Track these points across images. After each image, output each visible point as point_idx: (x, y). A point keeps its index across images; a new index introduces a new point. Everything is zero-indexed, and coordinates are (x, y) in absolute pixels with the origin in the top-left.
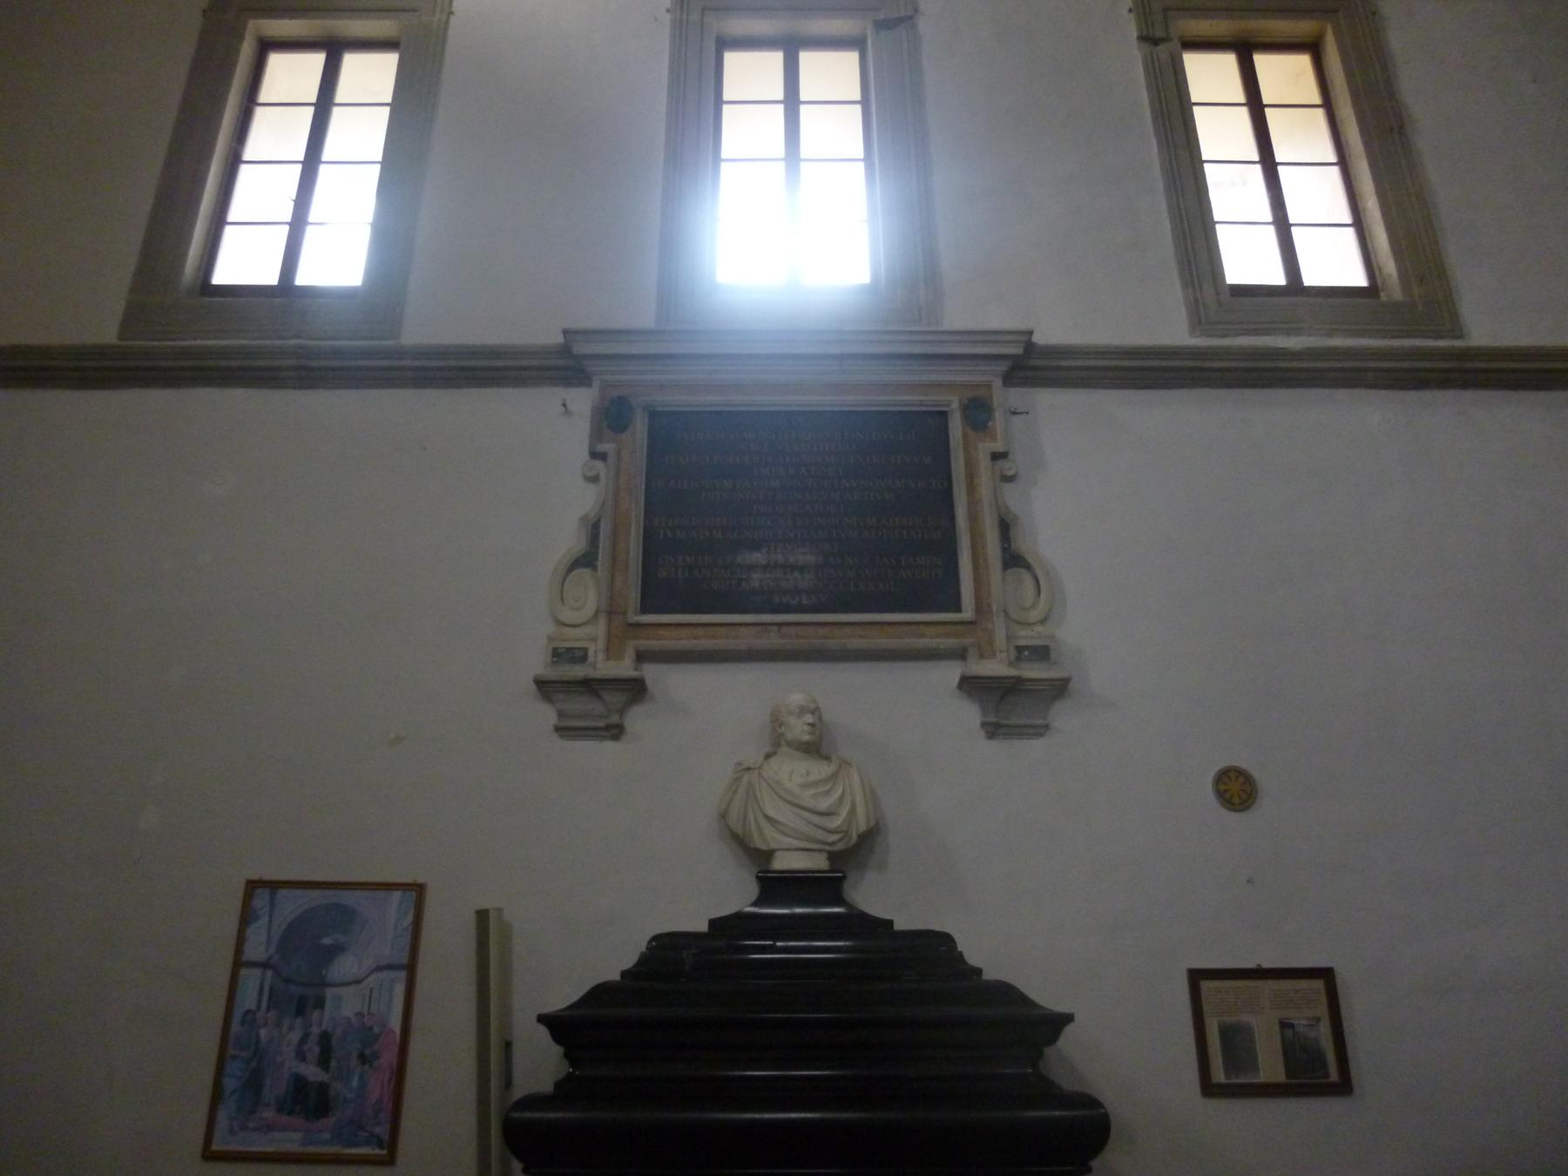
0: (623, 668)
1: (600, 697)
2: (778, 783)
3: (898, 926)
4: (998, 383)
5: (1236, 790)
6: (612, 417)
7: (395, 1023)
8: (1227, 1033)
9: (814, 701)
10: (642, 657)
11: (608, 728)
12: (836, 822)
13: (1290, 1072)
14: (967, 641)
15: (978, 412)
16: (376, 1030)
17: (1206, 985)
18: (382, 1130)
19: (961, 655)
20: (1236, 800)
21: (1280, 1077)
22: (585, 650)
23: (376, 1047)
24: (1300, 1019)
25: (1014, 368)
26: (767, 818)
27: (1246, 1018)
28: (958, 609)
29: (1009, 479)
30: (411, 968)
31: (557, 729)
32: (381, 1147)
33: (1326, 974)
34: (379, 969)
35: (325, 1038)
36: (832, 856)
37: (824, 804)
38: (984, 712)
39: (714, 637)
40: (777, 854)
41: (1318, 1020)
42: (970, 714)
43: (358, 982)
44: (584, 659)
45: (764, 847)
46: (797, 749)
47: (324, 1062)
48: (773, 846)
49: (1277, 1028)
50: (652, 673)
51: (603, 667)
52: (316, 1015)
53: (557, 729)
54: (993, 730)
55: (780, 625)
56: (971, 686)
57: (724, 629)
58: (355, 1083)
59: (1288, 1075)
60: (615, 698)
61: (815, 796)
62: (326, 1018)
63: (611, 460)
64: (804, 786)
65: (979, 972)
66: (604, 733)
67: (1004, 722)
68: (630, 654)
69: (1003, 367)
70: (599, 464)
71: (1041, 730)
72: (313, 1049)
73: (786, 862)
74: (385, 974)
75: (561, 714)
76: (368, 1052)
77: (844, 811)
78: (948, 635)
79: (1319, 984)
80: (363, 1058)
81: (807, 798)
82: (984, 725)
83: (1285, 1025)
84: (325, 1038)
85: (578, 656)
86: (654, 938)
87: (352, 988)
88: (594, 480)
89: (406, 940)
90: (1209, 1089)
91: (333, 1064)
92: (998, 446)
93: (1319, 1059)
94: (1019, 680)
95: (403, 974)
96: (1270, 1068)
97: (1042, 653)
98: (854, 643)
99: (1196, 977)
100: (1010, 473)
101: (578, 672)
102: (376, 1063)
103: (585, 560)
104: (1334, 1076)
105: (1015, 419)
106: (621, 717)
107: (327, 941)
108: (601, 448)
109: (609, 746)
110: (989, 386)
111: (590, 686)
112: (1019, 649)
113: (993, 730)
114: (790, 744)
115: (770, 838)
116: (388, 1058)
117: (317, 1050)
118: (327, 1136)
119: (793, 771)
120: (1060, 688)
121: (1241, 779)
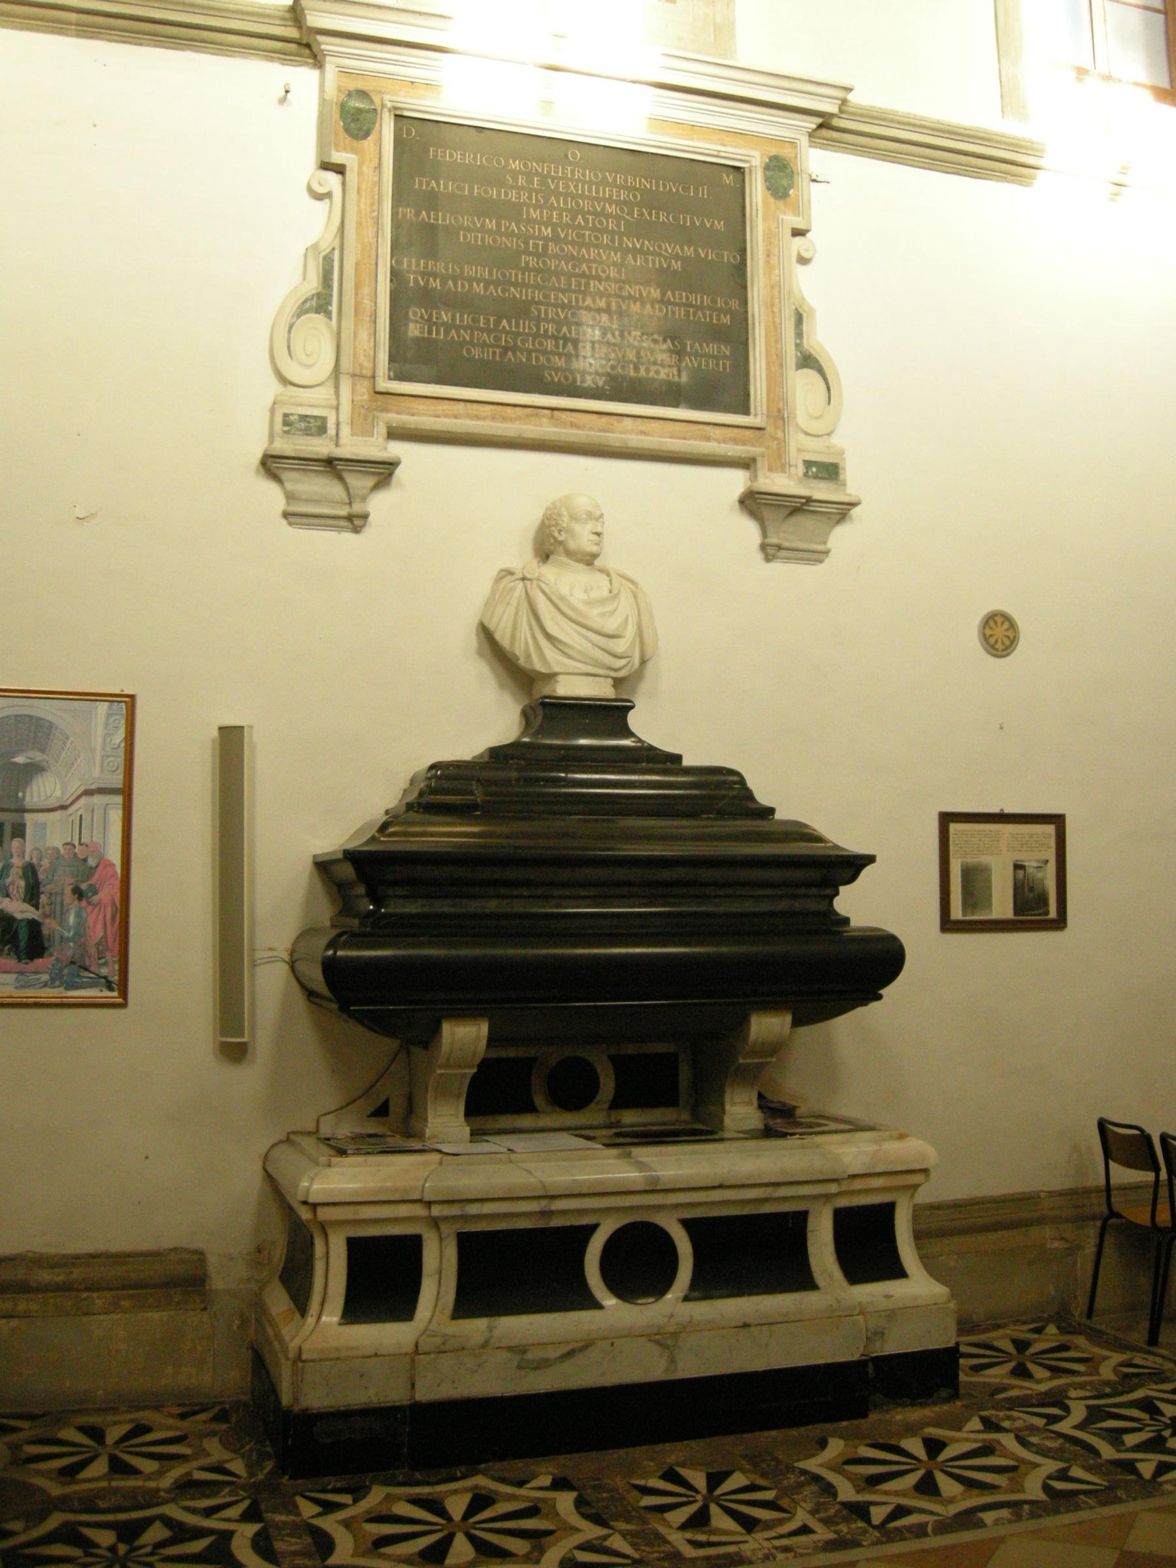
0: (374, 447)
1: (341, 479)
2: (562, 598)
3: (687, 762)
4: (804, 140)
5: (999, 634)
6: (353, 117)
7: (114, 855)
8: (968, 874)
9: (598, 506)
11: (350, 518)
12: (620, 646)
13: (1019, 908)
15: (781, 175)
16: (92, 862)
17: (954, 827)
18: (110, 970)
19: (747, 464)
20: (999, 646)
22: (324, 420)
23: (93, 881)
24: (1031, 864)
25: (821, 126)
26: (549, 637)
27: (985, 859)
28: (745, 409)
30: (127, 792)
31: (286, 515)
32: (111, 989)
33: (1058, 821)
34: (88, 793)
35: (30, 871)
36: (618, 683)
37: (610, 626)
38: (765, 534)
39: (478, 418)
40: (560, 678)
41: (1047, 862)
42: (749, 531)
43: (64, 807)
44: (322, 430)
45: (543, 670)
46: (577, 561)
47: (33, 894)
48: (557, 669)
49: (1012, 867)
51: (352, 446)
52: (16, 843)
53: (286, 515)
54: (769, 551)
55: (552, 409)
56: (752, 503)
57: (488, 407)
58: (72, 919)
59: (1015, 914)
60: (359, 482)
61: (603, 615)
62: (28, 849)
64: (590, 603)
65: (767, 813)
67: (786, 544)
68: (381, 430)
69: (811, 123)
70: (333, 179)
71: (818, 556)
72: (20, 885)
73: (570, 687)
74: (96, 799)
75: (290, 497)
76: (84, 886)
77: (630, 631)
78: (736, 441)
79: (1050, 829)
80: (79, 893)
81: (594, 616)
82: (763, 547)
83: (1018, 867)
84: (30, 871)
85: (318, 427)
86: (433, 767)
87: (57, 815)
89: (120, 760)
90: (948, 925)
91: (43, 899)
92: (800, 224)
93: (1043, 900)
94: (809, 500)
95: (119, 799)
96: (1002, 906)
98: (636, 441)
99: (947, 819)
101: (320, 447)
102: (95, 899)
103: (320, 303)
104: (1053, 914)
105: (813, 185)
107: (20, 759)
108: (337, 157)
109: (348, 536)
110: (793, 144)
111: (331, 465)
112: (808, 464)
113: (769, 551)
114: (569, 553)
115: (554, 660)
116: (108, 893)
117: (22, 883)
118: (45, 977)
119: (568, 581)
120: (842, 511)
121: (1006, 625)
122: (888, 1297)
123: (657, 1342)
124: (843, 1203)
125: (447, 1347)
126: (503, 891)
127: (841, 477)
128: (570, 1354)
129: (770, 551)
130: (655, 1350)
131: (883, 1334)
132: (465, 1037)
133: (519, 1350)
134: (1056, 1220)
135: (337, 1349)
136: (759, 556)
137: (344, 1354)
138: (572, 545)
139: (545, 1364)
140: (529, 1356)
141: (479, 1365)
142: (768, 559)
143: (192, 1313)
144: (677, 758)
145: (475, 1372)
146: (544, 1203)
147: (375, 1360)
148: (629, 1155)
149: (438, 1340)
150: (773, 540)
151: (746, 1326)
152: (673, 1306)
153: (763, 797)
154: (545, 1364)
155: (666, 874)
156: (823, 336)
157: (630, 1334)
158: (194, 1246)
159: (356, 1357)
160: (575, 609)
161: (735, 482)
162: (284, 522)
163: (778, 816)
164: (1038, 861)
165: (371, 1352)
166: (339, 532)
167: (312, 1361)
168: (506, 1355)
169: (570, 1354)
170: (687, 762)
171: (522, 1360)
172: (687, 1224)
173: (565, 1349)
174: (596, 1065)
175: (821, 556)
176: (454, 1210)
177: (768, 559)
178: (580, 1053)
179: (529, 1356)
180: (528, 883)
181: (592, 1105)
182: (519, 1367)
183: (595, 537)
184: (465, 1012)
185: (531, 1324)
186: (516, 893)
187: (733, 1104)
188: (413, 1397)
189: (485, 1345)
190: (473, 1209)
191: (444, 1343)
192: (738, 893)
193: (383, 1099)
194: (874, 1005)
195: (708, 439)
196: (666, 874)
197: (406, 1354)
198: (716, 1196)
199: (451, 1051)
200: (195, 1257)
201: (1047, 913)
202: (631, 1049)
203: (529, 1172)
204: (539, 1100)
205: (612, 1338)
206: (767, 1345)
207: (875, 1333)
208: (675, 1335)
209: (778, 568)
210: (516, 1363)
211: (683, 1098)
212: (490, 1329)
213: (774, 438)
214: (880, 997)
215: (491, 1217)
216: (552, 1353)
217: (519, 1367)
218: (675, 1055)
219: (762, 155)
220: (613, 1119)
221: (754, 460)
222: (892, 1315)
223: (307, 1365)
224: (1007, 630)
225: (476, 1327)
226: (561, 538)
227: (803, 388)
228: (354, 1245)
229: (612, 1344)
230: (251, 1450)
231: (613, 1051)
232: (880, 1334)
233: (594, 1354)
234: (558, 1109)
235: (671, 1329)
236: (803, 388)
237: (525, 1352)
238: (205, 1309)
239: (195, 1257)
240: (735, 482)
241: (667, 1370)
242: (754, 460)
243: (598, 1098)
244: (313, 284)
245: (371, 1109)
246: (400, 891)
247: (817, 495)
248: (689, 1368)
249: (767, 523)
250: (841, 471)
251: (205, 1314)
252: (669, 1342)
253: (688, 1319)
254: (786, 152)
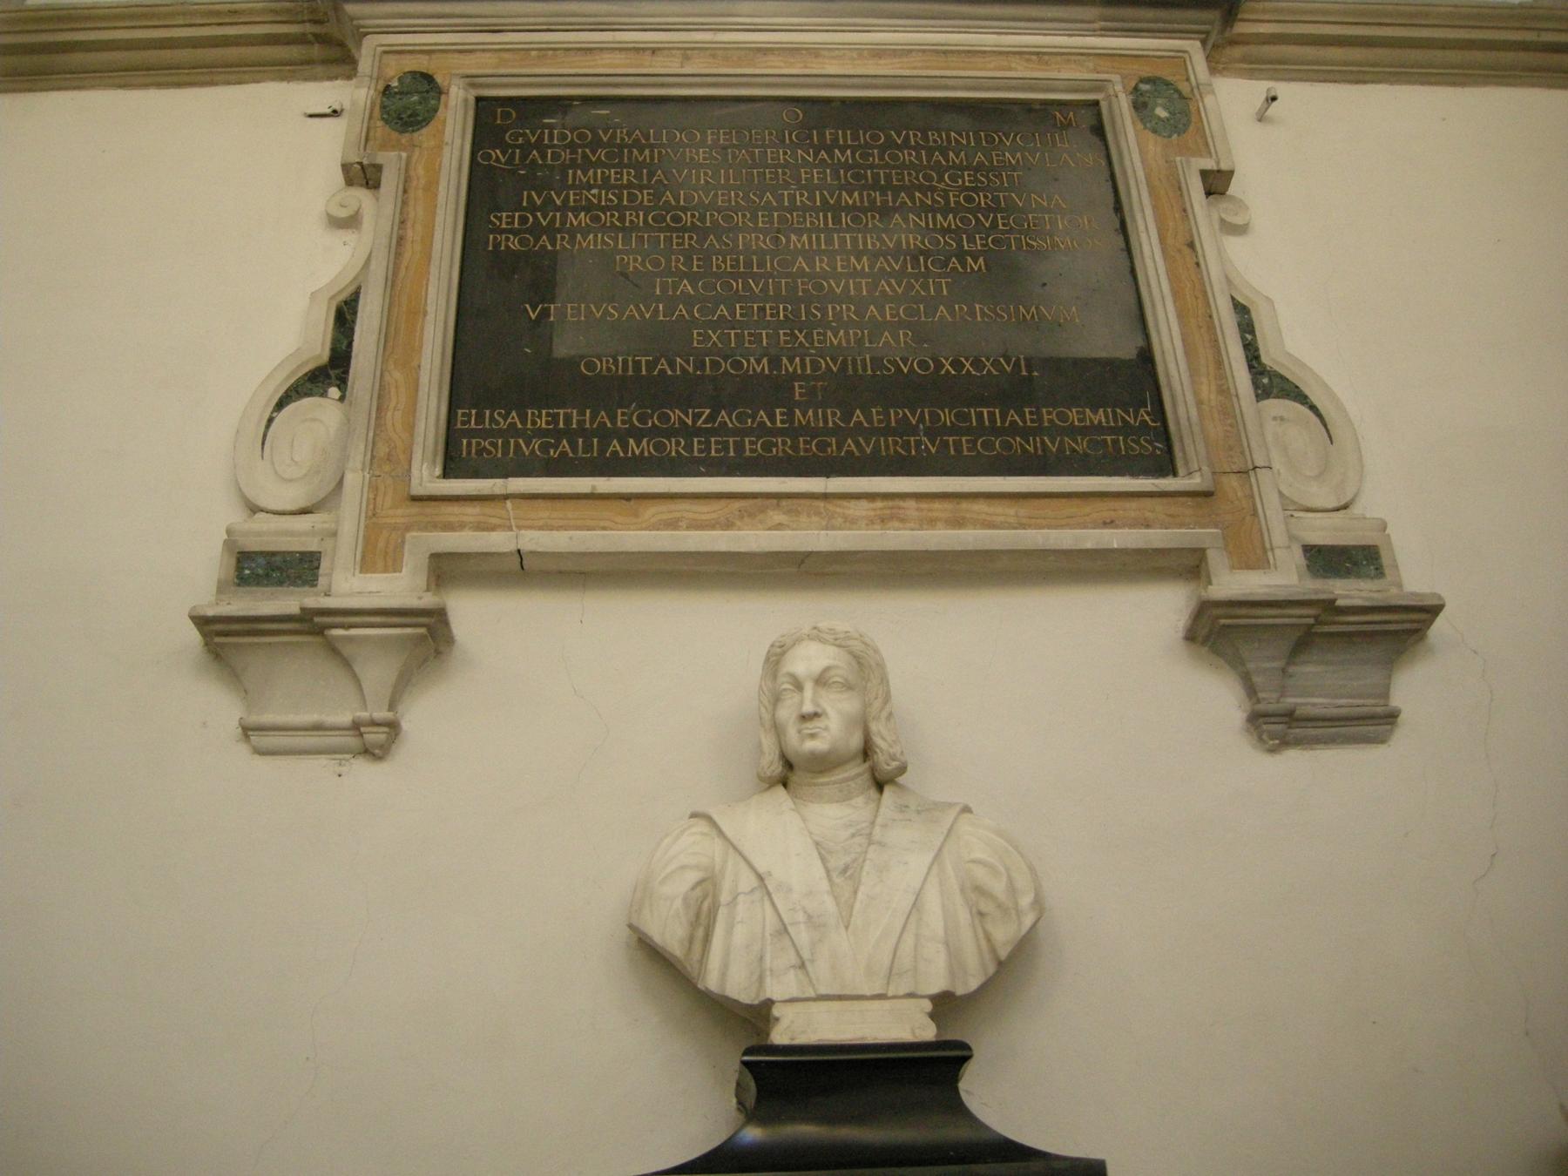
0: (401, 587)
6: (407, 105)
10: (447, 570)
29: (1240, 230)
38: (1251, 691)
50: (473, 614)
63: (390, 181)
71: (1373, 723)
85: (299, 568)
88: (350, 223)
97: (1355, 559)
100: (1238, 220)
103: (332, 372)
106: (392, 706)
120: (1405, 627)
150: (1271, 701)
156: (1293, 341)
162: (243, 749)
209: (1294, 758)
219: (1124, 77)
227: (1275, 428)
236: (1275, 428)
244: (320, 351)
254: (1166, 73)
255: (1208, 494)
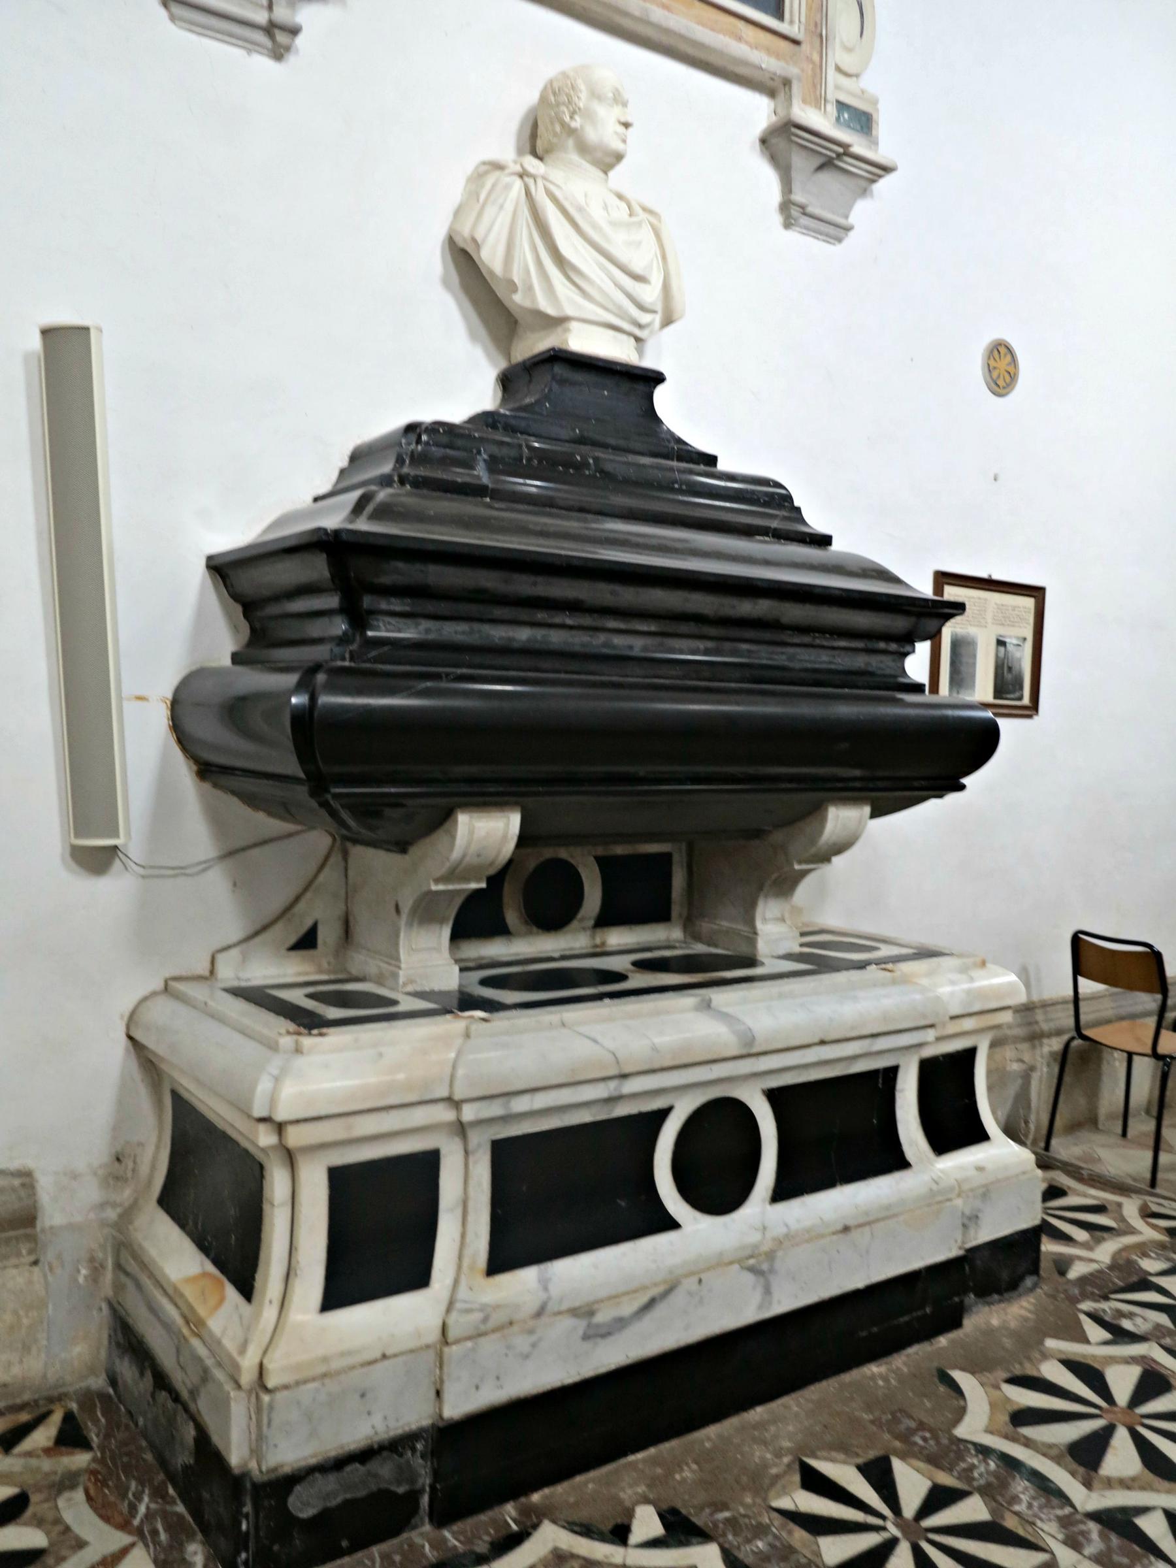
2: (580, 209)
11: (270, 29)
14: (792, 71)
21: (989, 697)
33: (1037, 593)
40: (574, 325)
41: (1025, 639)
45: (551, 311)
48: (569, 311)
49: (994, 642)
56: (783, 142)
59: (995, 697)
66: (260, 37)
67: (810, 209)
78: (769, 51)
79: (1029, 603)
83: (1001, 643)
104: (1026, 700)
109: (262, 63)
112: (841, 106)
114: (584, 149)
115: (563, 298)
122: (980, 1169)
123: (751, 1269)
124: (928, 1052)
125: (491, 1324)
126: (541, 616)
127: (874, 132)
128: (651, 1304)
129: (795, 212)
130: (749, 1278)
131: (977, 1217)
132: (488, 833)
133: (585, 1312)
134: (1017, 1040)
135: (325, 1359)
136: (777, 219)
137: (336, 1365)
138: (592, 135)
139: (621, 1323)
140: (601, 1317)
141: (534, 1345)
142: (787, 225)
143: (14, 1271)
144: (711, 460)
145: (527, 1357)
146: (612, 1085)
147: (386, 1363)
148: (707, 1005)
149: (478, 1316)
151: (846, 1229)
152: (759, 1214)
153: (816, 522)
154: (621, 1323)
155: (747, 608)
157: (720, 1263)
158: (15, 1165)
159: (352, 1368)
160: (595, 226)
161: (759, 112)
163: (836, 546)
164: (1018, 638)
165: (377, 1354)
166: (249, 51)
167: (286, 1387)
168: (568, 1322)
169: (651, 1304)
170: (722, 466)
171: (589, 1326)
172: (773, 1096)
173: (644, 1299)
174: (580, 870)
175: (840, 233)
176: (494, 1109)
177: (787, 225)
178: (563, 853)
179: (601, 1317)
180: (574, 607)
181: (575, 924)
182: (586, 1337)
183: (621, 129)
184: (486, 798)
185: (596, 1267)
186: (558, 620)
187: (765, 920)
188: (441, 1417)
189: (540, 1313)
190: (521, 1105)
191: (485, 1320)
192: (818, 642)
193: (308, 923)
194: (952, 798)
195: (739, 39)
196: (747, 608)
197: (428, 1347)
198: (811, 1055)
199: (464, 856)
200: (17, 1182)
201: (1020, 698)
202: (619, 850)
203: (595, 1041)
204: (512, 917)
205: (701, 1271)
206: (867, 1252)
207: (970, 1219)
208: (770, 1256)
209: (794, 238)
210: (580, 1332)
211: (676, 910)
212: (544, 1284)
213: (809, 60)
214: (962, 787)
215: (537, 1114)
216: (628, 1308)
217: (586, 1337)
218: (667, 858)
220: (598, 941)
221: (787, 83)
222: (986, 1193)
223: (279, 1396)
224: (1009, 364)
225: (524, 1282)
226: (573, 124)
228: (338, 1177)
229: (700, 1281)
230: (149, 1516)
231: (600, 851)
232: (971, 1220)
233: (678, 1299)
234: (535, 929)
235: (765, 1248)
237: (591, 1313)
238: (35, 1263)
239: (17, 1182)
240: (759, 112)
241: (760, 1307)
242: (787, 83)
243: (579, 916)
245: (293, 939)
246: (397, 605)
247: (857, 149)
248: (785, 1301)
249: (794, 174)
250: (874, 126)
251: (36, 1269)
252: (765, 1267)
253: (784, 1230)
255: (796, 42)
